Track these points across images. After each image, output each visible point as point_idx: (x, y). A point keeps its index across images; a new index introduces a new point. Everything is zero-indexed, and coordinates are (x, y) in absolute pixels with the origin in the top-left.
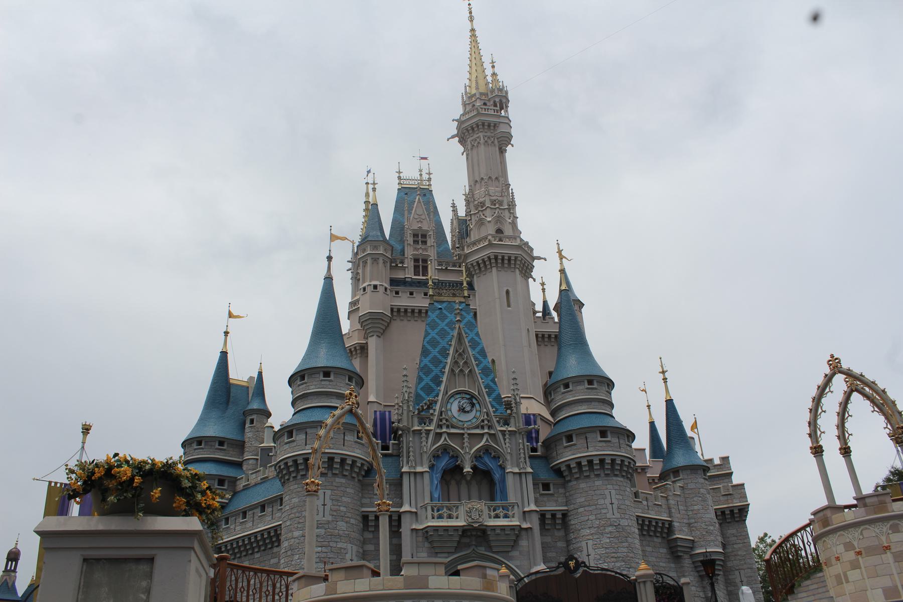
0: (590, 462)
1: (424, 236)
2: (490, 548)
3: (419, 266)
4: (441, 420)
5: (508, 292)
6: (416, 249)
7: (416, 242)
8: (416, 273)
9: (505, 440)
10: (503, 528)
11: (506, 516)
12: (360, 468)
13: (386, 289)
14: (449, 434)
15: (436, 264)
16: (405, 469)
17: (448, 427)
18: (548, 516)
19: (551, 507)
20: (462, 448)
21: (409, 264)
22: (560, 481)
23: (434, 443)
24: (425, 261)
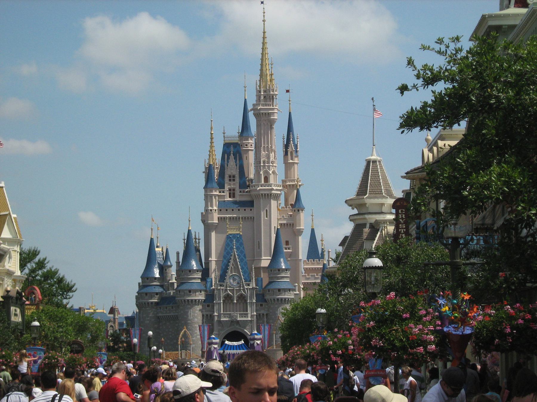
0: (274, 300)
1: (234, 176)
2: (240, 326)
3: (231, 193)
4: (227, 285)
5: (267, 211)
6: (230, 185)
7: (230, 180)
8: (230, 197)
9: (247, 291)
10: (244, 321)
11: (245, 317)
12: (201, 302)
13: (216, 210)
14: (229, 290)
15: (239, 191)
16: (214, 302)
17: (229, 287)
18: (261, 314)
19: (262, 312)
20: (233, 294)
21: (227, 194)
22: (266, 303)
23: (225, 293)
24: (234, 190)
